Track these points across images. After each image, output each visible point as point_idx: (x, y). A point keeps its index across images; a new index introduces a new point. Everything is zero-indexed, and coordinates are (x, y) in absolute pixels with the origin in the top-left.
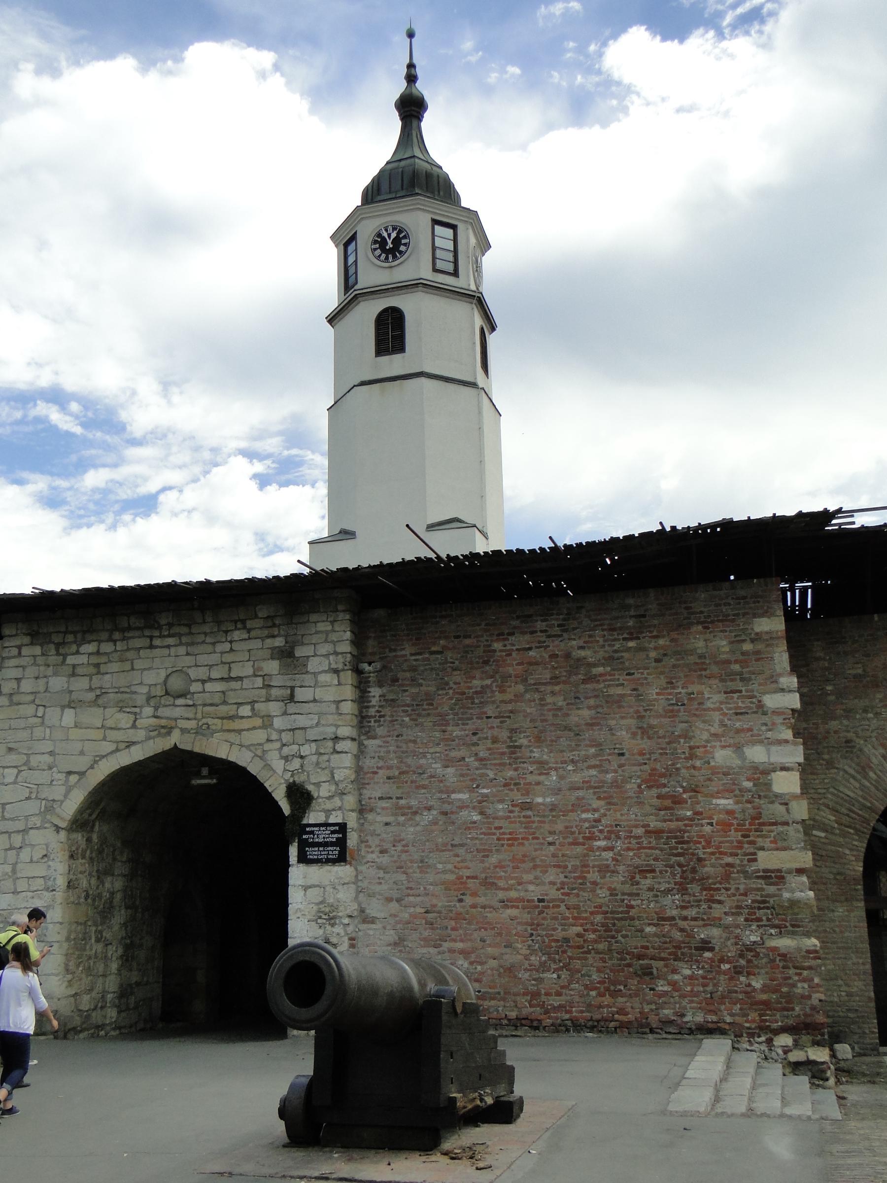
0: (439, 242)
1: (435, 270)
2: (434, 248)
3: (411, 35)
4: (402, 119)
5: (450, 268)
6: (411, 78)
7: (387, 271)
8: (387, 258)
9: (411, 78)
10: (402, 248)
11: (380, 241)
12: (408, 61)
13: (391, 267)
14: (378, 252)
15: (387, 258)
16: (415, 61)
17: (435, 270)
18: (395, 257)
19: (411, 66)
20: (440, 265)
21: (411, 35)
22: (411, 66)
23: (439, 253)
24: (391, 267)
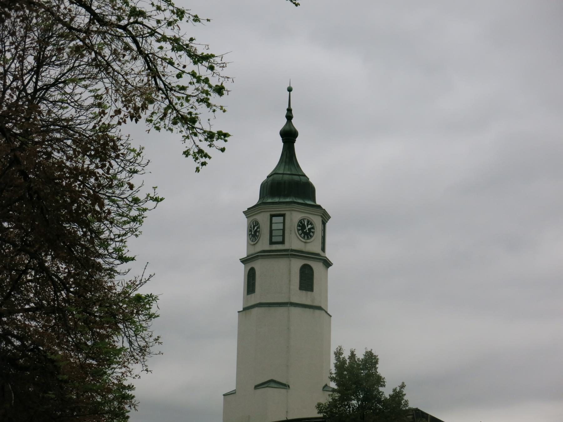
3: (290, 90)
6: (289, 117)
7: (303, 244)
8: (304, 237)
9: (289, 117)
10: (311, 234)
11: (301, 226)
12: (287, 107)
13: (305, 243)
14: (300, 232)
15: (304, 237)
16: (292, 107)
18: (308, 238)
19: (289, 110)
21: (290, 90)
22: (289, 110)
24: (305, 243)
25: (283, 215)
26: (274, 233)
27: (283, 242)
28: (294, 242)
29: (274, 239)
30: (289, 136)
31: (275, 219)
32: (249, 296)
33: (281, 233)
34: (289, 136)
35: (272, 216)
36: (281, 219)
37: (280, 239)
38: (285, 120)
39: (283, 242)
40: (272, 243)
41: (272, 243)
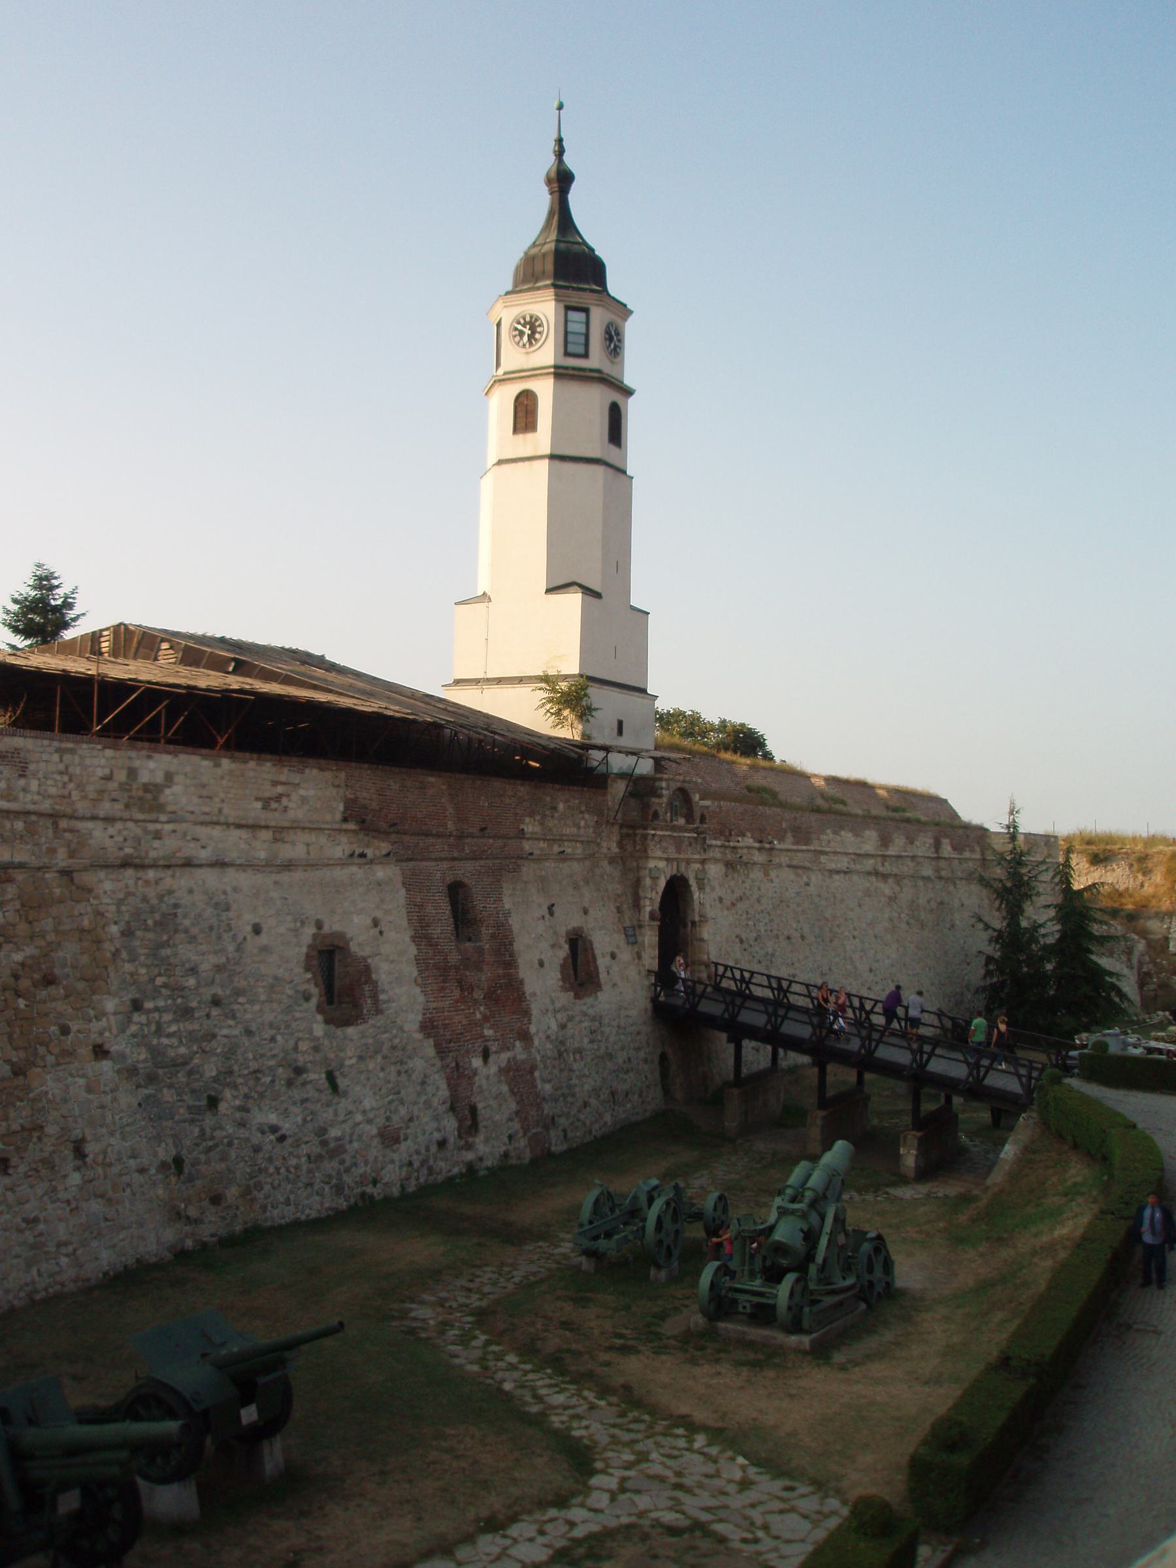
6: (560, 153)
9: (560, 153)
19: (560, 141)
21: (560, 107)
22: (560, 141)
25: (586, 311)
26: (571, 338)
27: (586, 355)
28: (596, 360)
29: (571, 349)
30: (561, 180)
31: (573, 316)
32: (521, 437)
33: (582, 340)
34: (562, 181)
35: (568, 308)
36: (581, 316)
37: (581, 350)
39: (586, 355)
40: (567, 354)
41: (567, 354)
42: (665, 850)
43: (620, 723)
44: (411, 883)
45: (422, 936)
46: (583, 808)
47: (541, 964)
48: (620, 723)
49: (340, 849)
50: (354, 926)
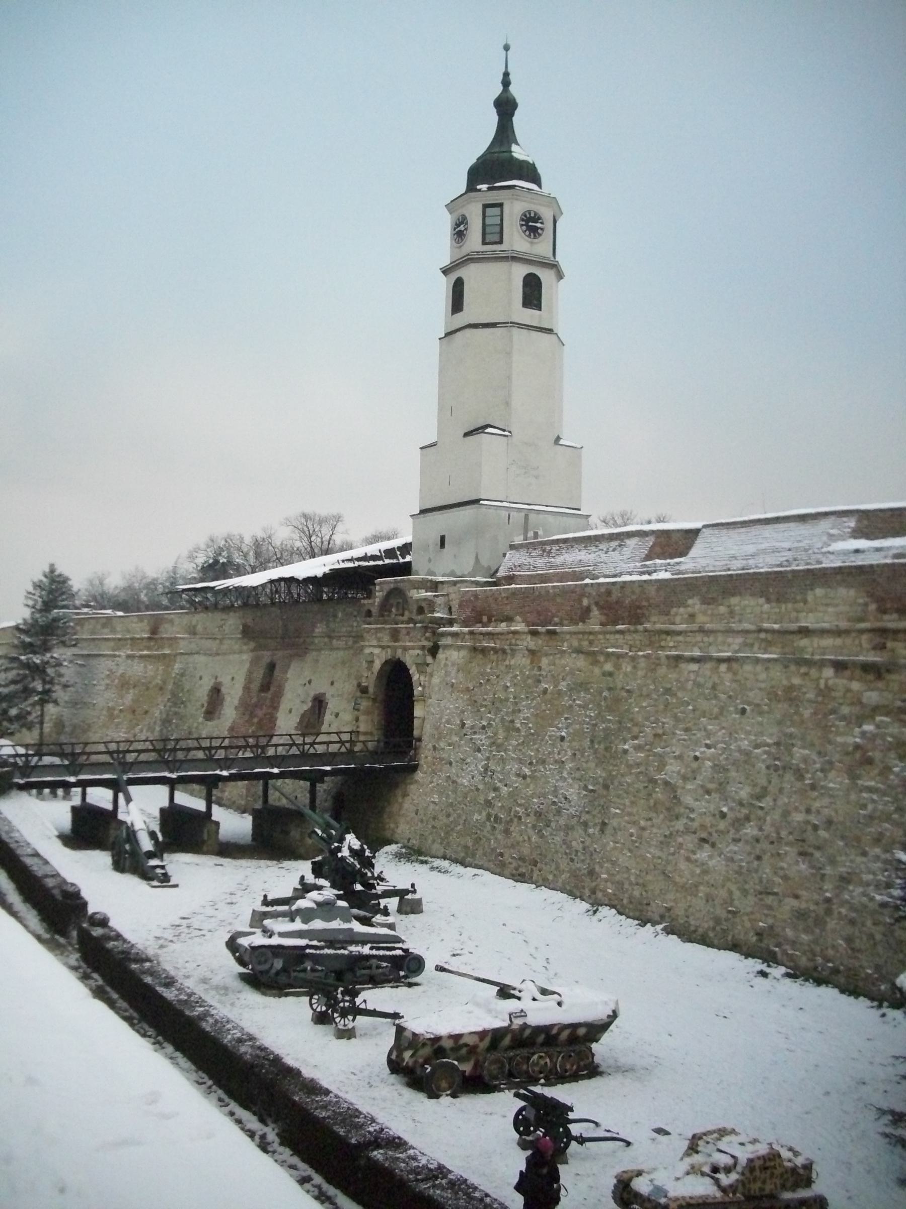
0: (489, 221)
1: (484, 243)
2: (484, 226)
3: (507, 48)
4: (499, 115)
5: (496, 238)
6: (506, 83)
9: (506, 83)
12: (504, 70)
17: (484, 243)
19: (506, 74)
20: (489, 238)
21: (507, 48)
22: (506, 74)
23: (488, 230)
30: (506, 107)
34: (506, 107)
38: (501, 88)
42: (379, 640)
43: (443, 539)
44: (255, 662)
45: (247, 688)
46: (355, 613)
47: (290, 711)
48: (443, 539)
49: (236, 647)
50: (225, 680)
